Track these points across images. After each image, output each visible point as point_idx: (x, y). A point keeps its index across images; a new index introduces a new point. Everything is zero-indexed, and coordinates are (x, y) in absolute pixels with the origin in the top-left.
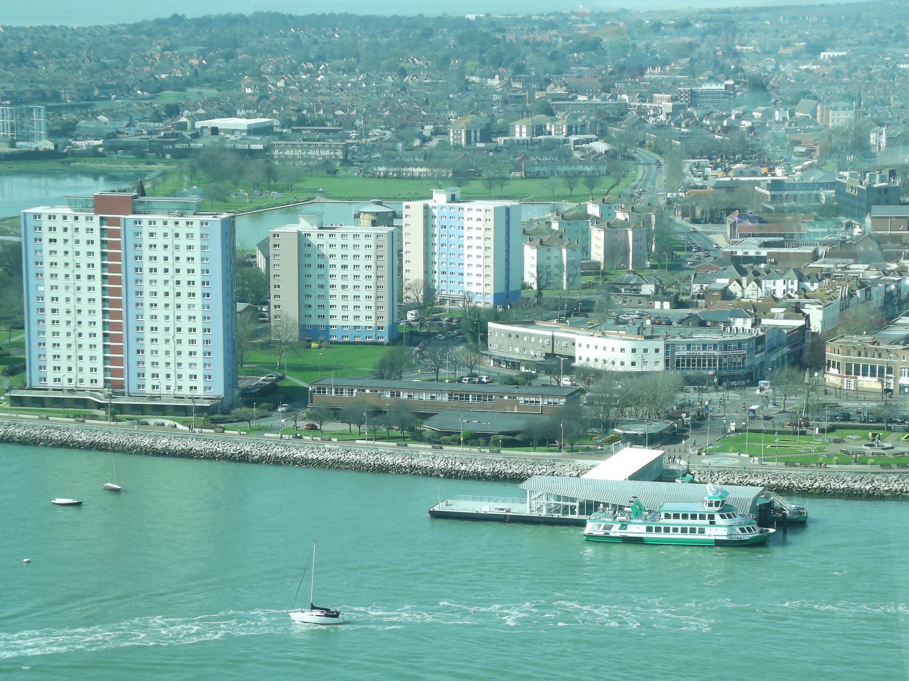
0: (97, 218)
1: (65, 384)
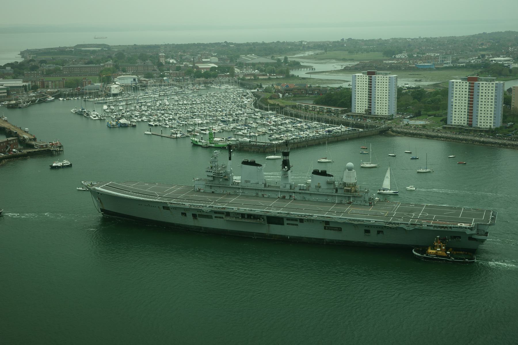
0: (468, 83)
1: (457, 124)
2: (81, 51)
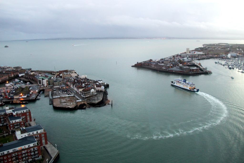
2: (220, 45)
